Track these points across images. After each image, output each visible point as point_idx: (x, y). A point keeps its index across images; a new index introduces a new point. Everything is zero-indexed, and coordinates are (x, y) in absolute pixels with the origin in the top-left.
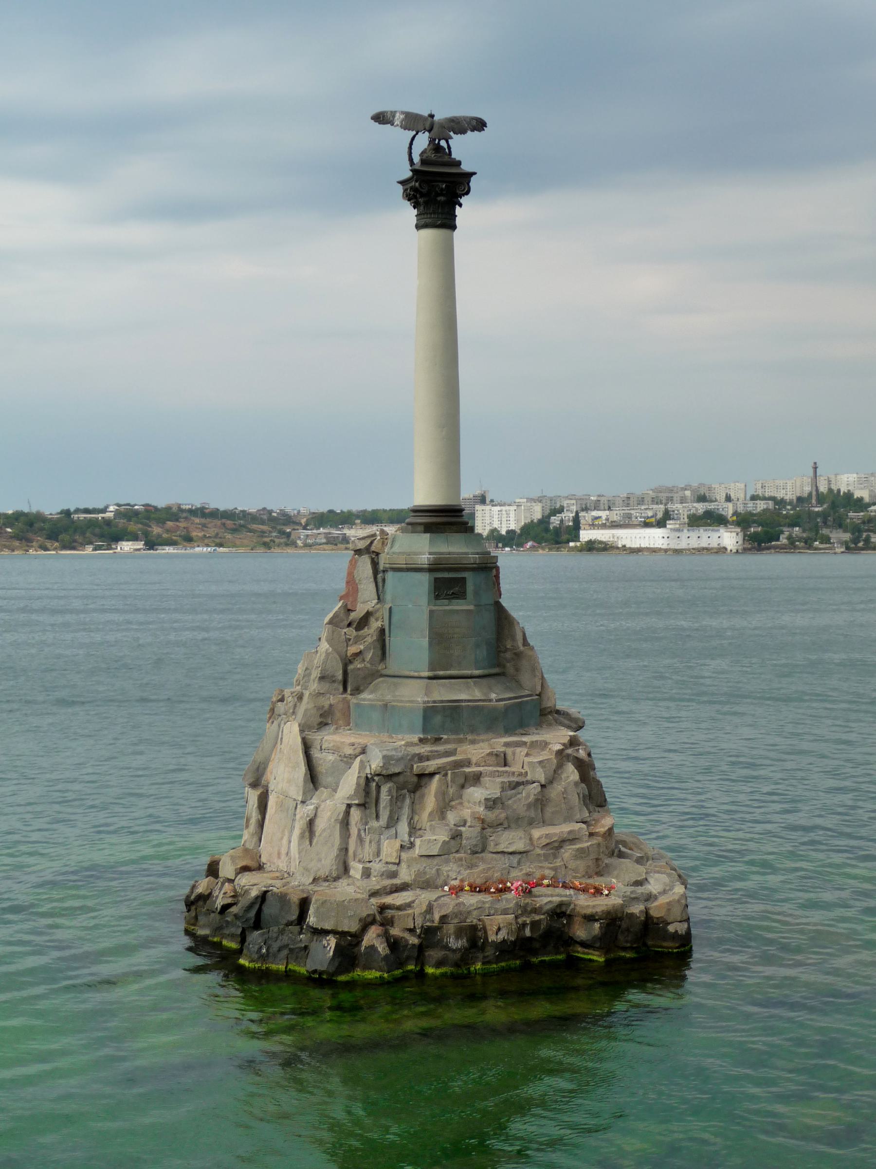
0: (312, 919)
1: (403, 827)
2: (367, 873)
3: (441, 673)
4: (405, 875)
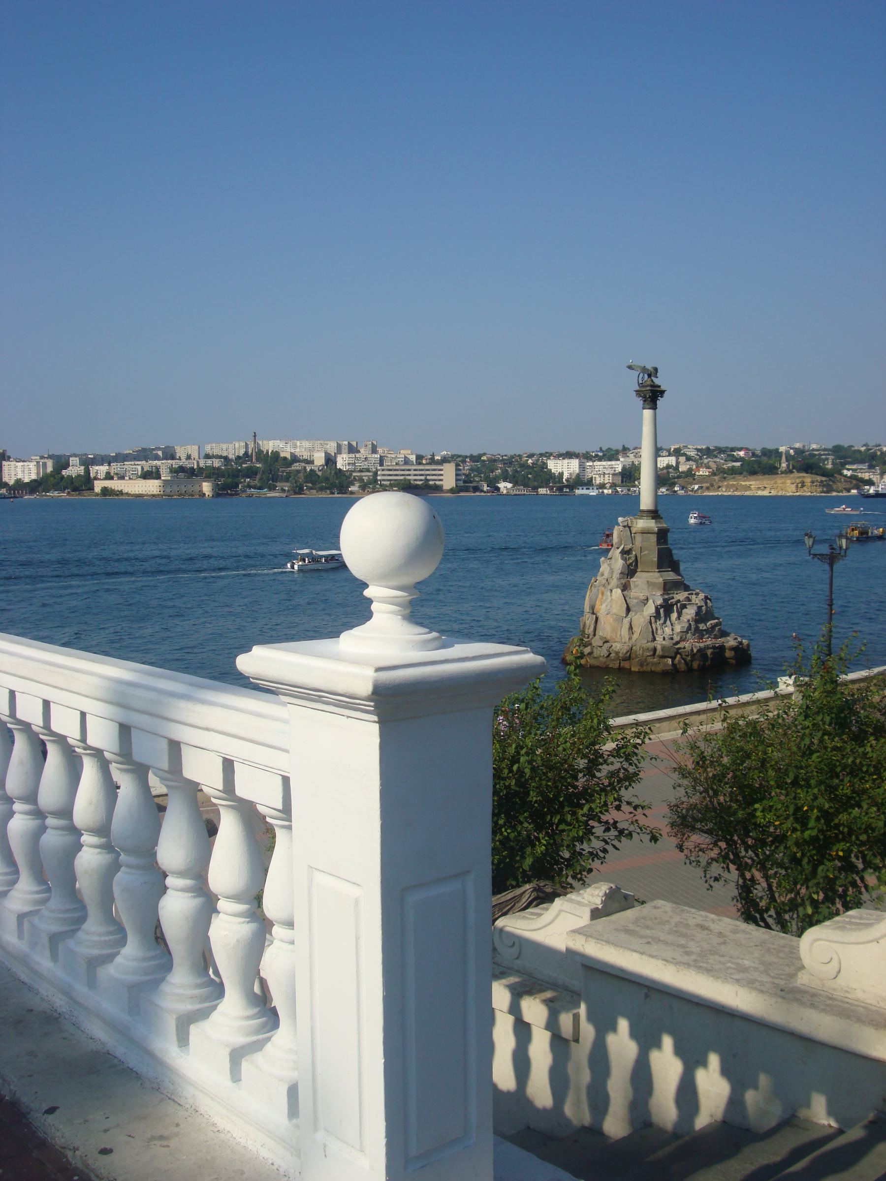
0: (659, 652)
1: (668, 622)
2: (664, 639)
4: (676, 638)
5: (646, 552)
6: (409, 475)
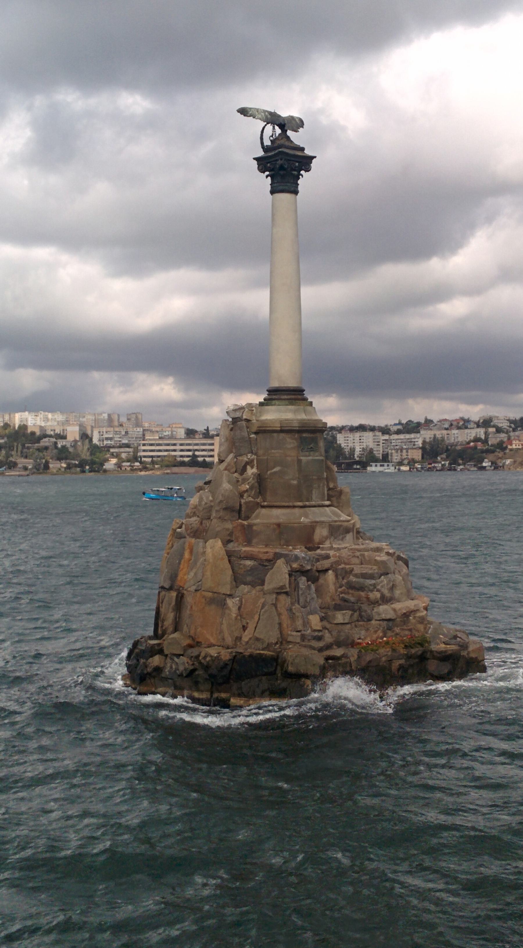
3: (307, 503)
5: (277, 469)
6: (175, 450)
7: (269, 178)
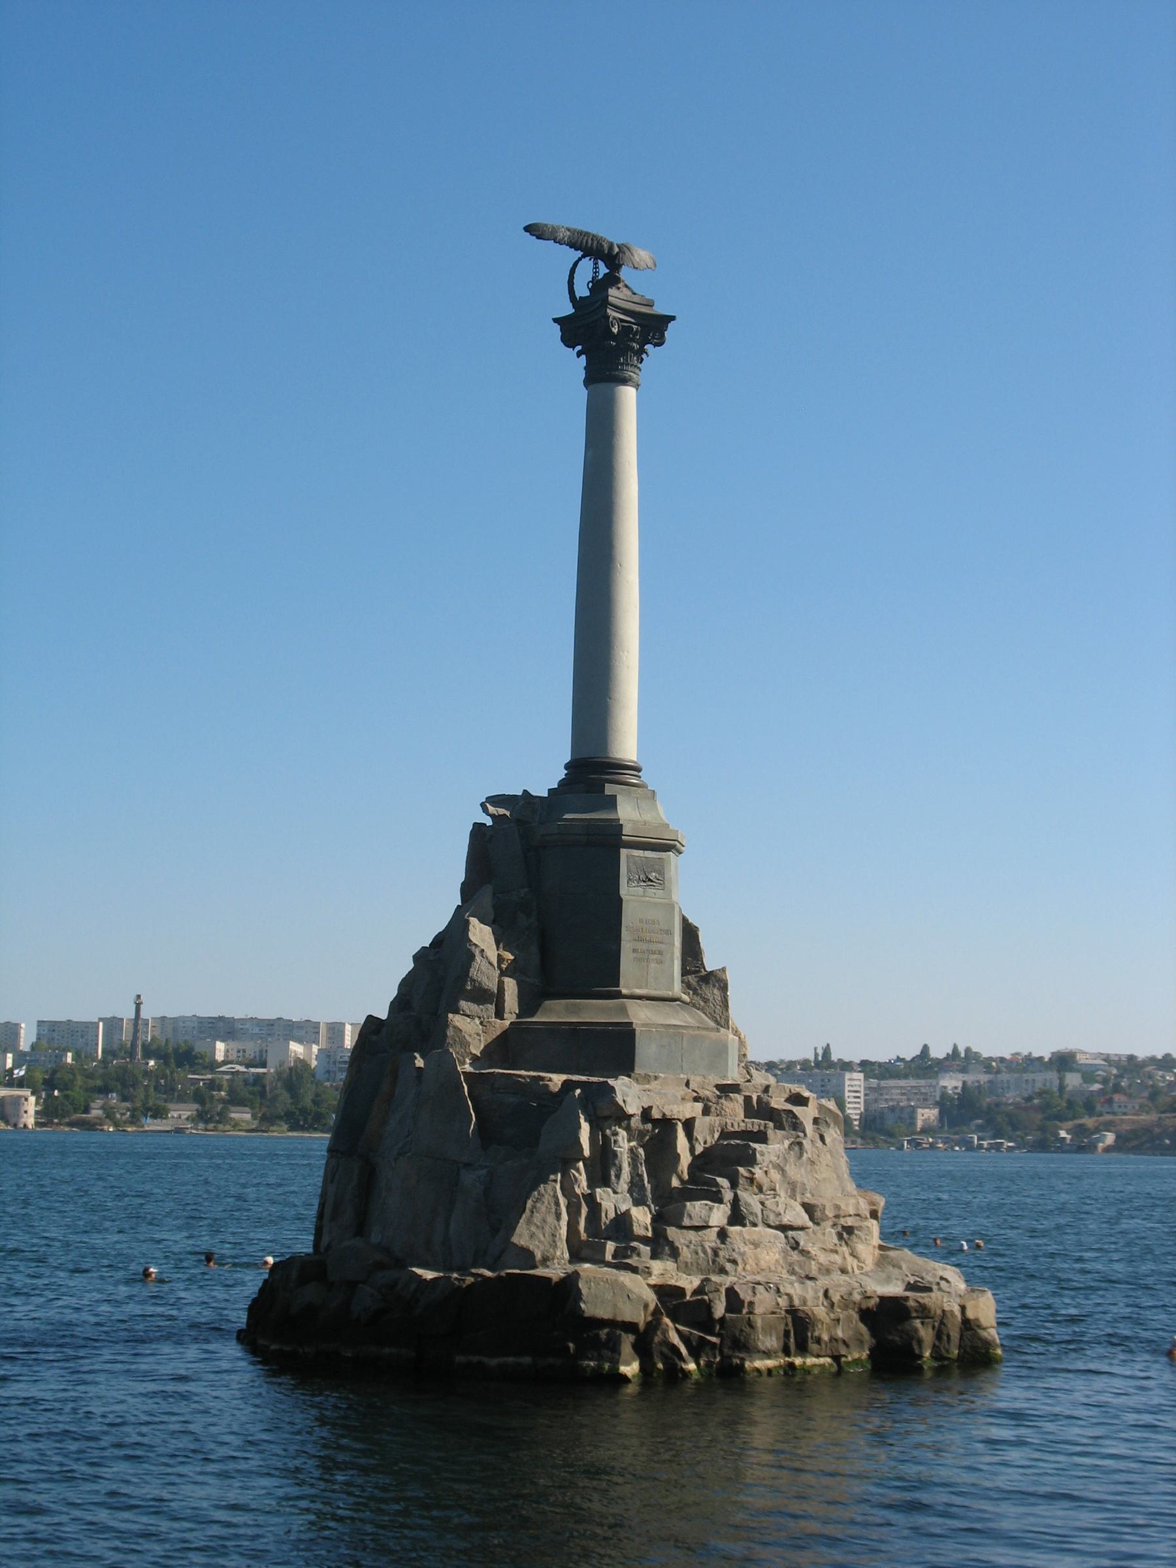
3: (638, 991)
7: (584, 357)
